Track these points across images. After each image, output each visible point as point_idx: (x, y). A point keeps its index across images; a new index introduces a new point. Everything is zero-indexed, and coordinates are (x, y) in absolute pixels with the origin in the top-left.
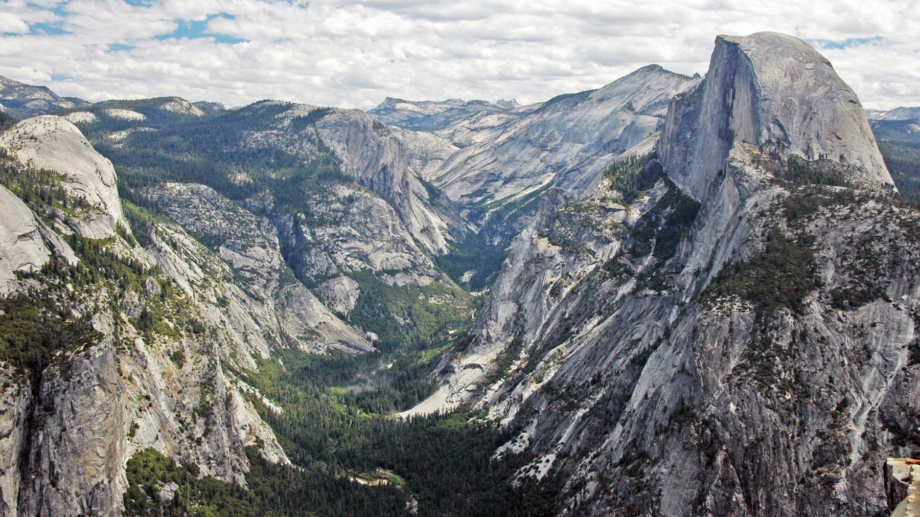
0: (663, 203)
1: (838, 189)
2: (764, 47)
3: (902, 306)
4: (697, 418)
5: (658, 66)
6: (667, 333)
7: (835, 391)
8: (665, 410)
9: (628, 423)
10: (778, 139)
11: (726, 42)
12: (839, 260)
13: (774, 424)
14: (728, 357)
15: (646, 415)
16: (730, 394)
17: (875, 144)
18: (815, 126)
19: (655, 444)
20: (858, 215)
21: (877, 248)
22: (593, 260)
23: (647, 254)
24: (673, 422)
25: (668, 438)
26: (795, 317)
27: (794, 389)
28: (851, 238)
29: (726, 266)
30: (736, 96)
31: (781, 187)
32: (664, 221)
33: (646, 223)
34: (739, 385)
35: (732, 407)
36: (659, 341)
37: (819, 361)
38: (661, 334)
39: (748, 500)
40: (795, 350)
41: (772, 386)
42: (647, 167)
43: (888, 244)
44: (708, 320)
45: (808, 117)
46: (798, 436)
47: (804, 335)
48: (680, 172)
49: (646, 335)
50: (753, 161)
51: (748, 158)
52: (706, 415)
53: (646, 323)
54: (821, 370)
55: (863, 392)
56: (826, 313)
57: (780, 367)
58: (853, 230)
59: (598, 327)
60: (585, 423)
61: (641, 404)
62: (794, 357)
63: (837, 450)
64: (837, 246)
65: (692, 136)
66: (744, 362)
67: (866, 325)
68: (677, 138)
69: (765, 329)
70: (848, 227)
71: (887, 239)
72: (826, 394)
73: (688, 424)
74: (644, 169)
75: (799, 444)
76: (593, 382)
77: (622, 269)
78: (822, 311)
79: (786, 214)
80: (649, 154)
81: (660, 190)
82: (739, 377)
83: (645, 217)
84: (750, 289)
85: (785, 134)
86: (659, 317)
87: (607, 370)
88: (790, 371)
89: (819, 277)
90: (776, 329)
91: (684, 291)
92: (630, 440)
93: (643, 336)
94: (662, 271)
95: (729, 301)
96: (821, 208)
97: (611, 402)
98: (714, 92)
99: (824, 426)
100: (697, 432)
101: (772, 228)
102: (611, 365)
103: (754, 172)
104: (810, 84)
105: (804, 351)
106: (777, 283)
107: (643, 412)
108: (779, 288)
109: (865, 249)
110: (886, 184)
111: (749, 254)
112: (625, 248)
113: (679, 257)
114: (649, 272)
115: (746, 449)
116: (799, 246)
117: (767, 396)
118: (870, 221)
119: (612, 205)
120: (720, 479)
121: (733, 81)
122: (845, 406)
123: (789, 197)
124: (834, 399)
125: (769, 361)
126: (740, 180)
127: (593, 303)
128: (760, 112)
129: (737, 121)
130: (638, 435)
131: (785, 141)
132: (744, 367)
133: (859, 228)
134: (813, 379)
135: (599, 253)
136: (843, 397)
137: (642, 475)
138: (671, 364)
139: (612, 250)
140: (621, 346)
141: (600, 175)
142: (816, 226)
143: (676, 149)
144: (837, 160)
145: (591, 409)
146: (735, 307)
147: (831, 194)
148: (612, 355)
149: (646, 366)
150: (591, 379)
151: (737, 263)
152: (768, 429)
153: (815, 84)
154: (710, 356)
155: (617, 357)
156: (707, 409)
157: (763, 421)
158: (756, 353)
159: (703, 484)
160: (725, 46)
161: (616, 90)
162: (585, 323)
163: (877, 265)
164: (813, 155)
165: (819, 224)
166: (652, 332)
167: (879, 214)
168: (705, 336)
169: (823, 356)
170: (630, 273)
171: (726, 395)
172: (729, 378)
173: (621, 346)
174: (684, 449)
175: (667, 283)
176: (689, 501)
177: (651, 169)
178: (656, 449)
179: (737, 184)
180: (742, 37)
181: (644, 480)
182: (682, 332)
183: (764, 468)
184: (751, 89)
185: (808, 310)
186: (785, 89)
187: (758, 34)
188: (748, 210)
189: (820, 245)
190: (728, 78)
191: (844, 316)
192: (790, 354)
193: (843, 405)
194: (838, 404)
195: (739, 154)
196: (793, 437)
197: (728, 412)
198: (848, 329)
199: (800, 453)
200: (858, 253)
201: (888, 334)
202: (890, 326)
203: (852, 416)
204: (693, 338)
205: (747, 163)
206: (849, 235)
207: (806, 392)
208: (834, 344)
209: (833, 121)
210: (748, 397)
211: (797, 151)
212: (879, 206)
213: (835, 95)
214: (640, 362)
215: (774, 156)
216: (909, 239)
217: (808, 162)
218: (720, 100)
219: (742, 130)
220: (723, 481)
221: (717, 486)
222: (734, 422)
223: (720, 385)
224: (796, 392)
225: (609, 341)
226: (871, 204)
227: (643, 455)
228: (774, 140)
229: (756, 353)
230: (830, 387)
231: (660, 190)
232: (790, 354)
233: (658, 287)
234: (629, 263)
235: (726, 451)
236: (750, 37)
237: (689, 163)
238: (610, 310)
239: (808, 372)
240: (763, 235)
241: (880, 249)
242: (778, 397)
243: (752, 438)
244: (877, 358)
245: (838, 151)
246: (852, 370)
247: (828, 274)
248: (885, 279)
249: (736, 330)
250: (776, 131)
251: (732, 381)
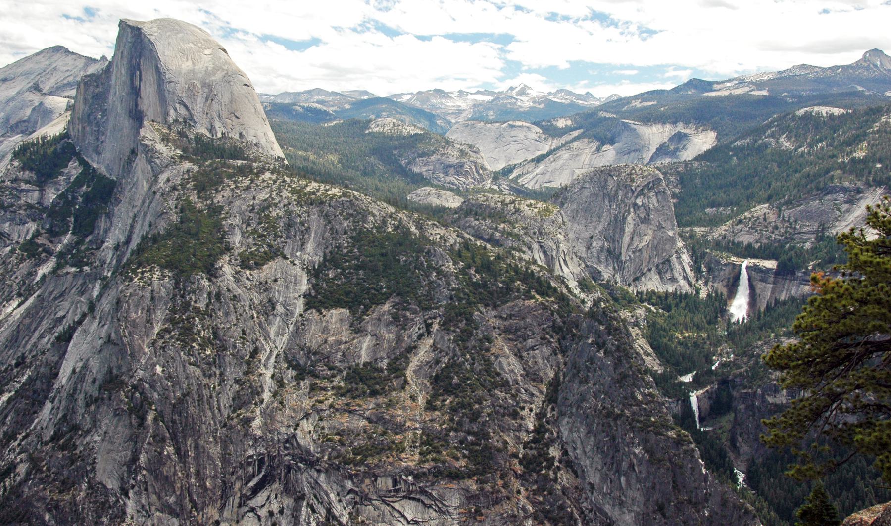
0: (79, 182)
1: (239, 163)
3: (297, 262)
4: (126, 384)
5: (63, 47)
6: (92, 307)
7: (248, 341)
8: (94, 381)
9: (57, 399)
10: (184, 118)
11: (129, 26)
12: (244, 226)
13: (198, 378)
14: (152, 324)
15: (75, 389)
16: (156, 357)
17: (267, 123)
18: (216, 106)
19: (86, 415)
20: (257, 185)
21: (274, 214)
22: (8, 242)
23: (65, 232)
24: (102, 391)
25: (98, 407)
26: (210, 280)
27: (213, 345)
28: (253, 206)
29: (144, 238)
30: (143, 78)
32: (80, 199)
33: (62, 203)
34: (163, 348)
35: (159, 369)
36: (84, 315)
37: (233, 317)
38: (85, 309)
39: (178, 451)
40: (212, 309)
41: (194, 345)
42: (59, 147)
43: (283, 210)
44: (131, 290)
45: (210, 98)
46: (219, 386)
47: (218, 296)
48: (93, 151)
49: (71, 311)
50: (163, 140)
51: (158, 138)
52: (135, 380)
53: (69, 299)
54: (235, 325)
55: (270, 339)
56: (236, 274)
57: (200, 326)
58: (254, 198)
59: (19, 309)
60: (10, 406)
61: (70, 378)
62: (211, 316)
63: (252, 393)
64: (241, 213)
65: (103, 116)
66: (166, 326)
67: (269, 281)
68: (88, 118)
69: (184, 294)
70: (250, 196)
71: (282, 205)
72: (241, 345)
73: (117, 392)
74: (56, 149)
75: (219, 394)
76: (17, 365)
77: (40, 249)
78: (233, 272)
79: (195, 187)
80: (60, 134)
81: (73, 169)
82: (163, 341)
83: (60, 197)
84: (168, 259)
85: (190, 114)
86: (81, 293)
87: (31, 351)
88: (209, 329)
89: (229, 243)
90: (194, 292)
91: (106, 266)
92: (60, 415)
93: (68, 313)
94: (82, 248)
95: (149, 271)
96: (226, 180)
97: (38, 382)
98: (121, 74)
99: (241, 374)
100: (127, 397)
101: (184, 200)
102: (35, 345)
104: (209, 68)
105: (219, 310)
106: (192, 251)
107: (72, 386)
108: (194, 255)
109: (265, 215)
110: (278, 157)
111: (165, 225)
112: (42, 228)
113: (98, 233)
114: (69, 250)
115: (174, 406)
116: (210, 216)
117: (189, 354)
118: (267, 190)
119: (24, 186)
120: (151, 437)
121: (139, 64)
122: (257, 354)
123: (198, 172)
124: (248, 349)
125: (190, 322)
126: (152, 157)
127: (11, 286)
128: (166, 93)
129: (146, 102)
130: (68, 410)
131: (191, 120)
132: (167, 330)
133: (259, 196)
134: (229, 334)
135: (15, 236)
136: (255, 346)
137: (75, 447)
138: (97, 337)
139: (28, 231)
140: (45, 324)
141: (9, 157)
142: (223, 197)
143: (88, 129)
145: (16, 392)
146: (155, 276)
147: (234, 168)
148: (36, 335)
149: (72, 342)
150: (14, 362)
151: (154, 235)
152: (192, 384)
153: (214, 68)
154: (134, 324)
155: (41, 337)
156: (135, 374)
157: (187, 378)
158: (177, 316)
159: (136, 443)
160: (129, 30)
161: (20, 70)
162: (4, 306)
163: (275, 228)
164: (216, 133)
165: (225, 195)
166: (76, 308)
167: (274, 184)
168: (129, 306)
169: (236, 312)
170: (50, 253)
171: (152, 359)
172: (154, 343)
173: (45, 324)
174: (116, 415)
175: (88, 260)
176: (123, 463)
177: (63, 149)
178: (88, 419)
179: (150, 161)
180: (145, 22)
181: (77, 452)
182: (106, 305)
183: (190, 419)
184: (156, 72)
185: (221, 272)
187: (159, 20)
188: (161, 185)
189: (227, 213)
190: (134, 61)
191: (251, 275)
192: (208, 313)
193: (255, 352)
194: (250, 352)
195: (149, 133)
196: (214, 388)
197: (155, 374)
198: (255, 286)
199: (222, 401)
200: (259, 218)
201: (287, 287)
202: (288, 280)
203: (263, 361)
204: (117, 309)
205: (158, 141)
206: (251, 204)
207: (223, 346)
208: (244, 301)
209: (231, 102)
210: (172, 358)
211: (202, 130)
212: (274, 177)
214: (65, 338)
215: (181, 134)
216: (299, 204)
217: (212, 140)
218: (128, 82)
219: (151, 110)
220: (154, 437)
221: (149, 444)
222: (161, 382)
223: (146, 350)
224: (215, 347)
225: (31, 323)
226: (268, 175)
227: (75, 428)
228: (181, 120)
229: (177, 316)
230: (244, 339)
231: (73, 169)
232: (208, 313)
233: (79, 264)
234: (47, 243)
235: (156, 410)
236: (152, 22)
237: (102, 142)
238: (30, 292)
239: (224, 328)
240: (176, 207)
241: (277, 214)
242: (199, 354)
243: (178, 394)
244: (280, 309)
245: (237, 129)
246: (260, 321)
247: (236, 239)
248: (283, 239)
249: (157, 297)
250: (182, 111)
251: (156, 345)
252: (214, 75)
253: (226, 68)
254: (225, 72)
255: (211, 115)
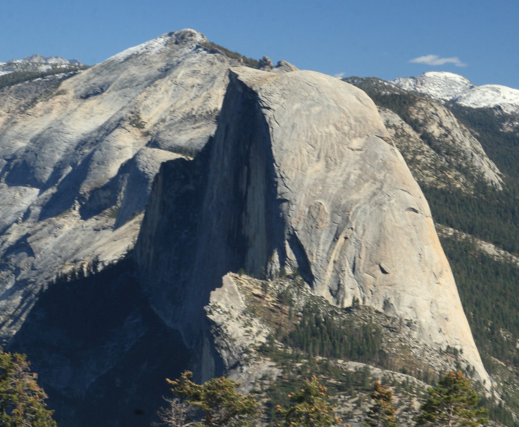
1: (352, 366)
2: (293, 104)
11: (241, 83)
18: (351, 250)
31: (271, 361)
103: (241, 332)
104: (352, 177)
110: (448, 347)
144: (380, 308)
153: (360, 176)
160: (240, 89)
164: (343, 299)
186: (315, 185)
205: (236, 314)
213: (386, 199)
245: (384, 292)
252: (358, 190)
253: (380, 176)
254: (378, 185)
255: (341, 266)
